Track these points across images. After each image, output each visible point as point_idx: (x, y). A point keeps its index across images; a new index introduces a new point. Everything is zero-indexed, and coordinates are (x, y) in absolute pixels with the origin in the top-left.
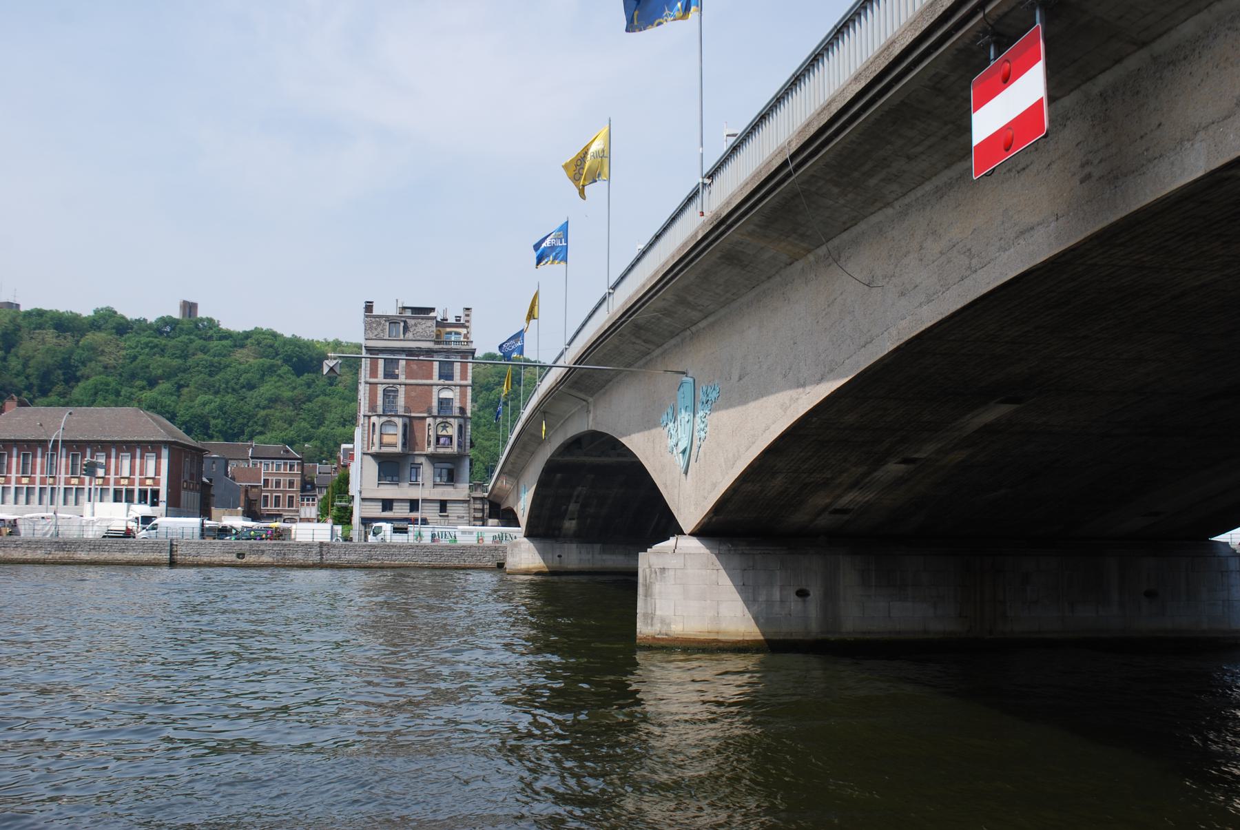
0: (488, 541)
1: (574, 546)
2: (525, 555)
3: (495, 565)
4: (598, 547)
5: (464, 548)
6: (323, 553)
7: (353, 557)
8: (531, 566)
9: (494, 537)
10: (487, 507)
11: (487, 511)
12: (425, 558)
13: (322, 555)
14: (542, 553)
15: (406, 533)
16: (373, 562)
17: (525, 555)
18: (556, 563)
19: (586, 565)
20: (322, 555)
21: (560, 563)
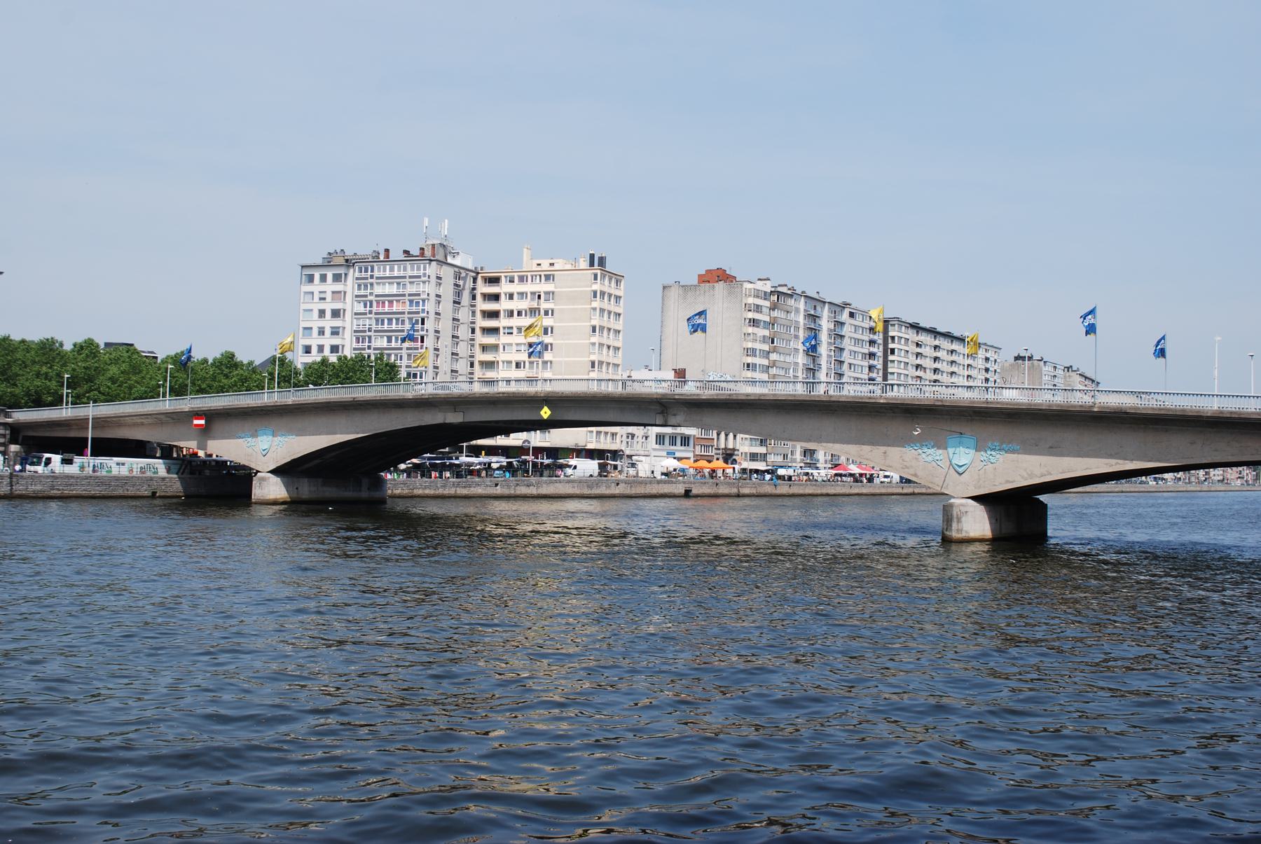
0: (89, 471)
1: (306, 480)
2: (272, 488)
3: (150, 494)
4: (320, 480)
5: (117, 478)
6: (14, 484)
7: (39, 488)
8: (278, 497)
9: (141, 468)
10: (8, 432)
11: (8, 437)
12: (97, 488)
13: (12, 486)
14: (287, 486)
15: (72, 464)
16: (55, 492)
17: (272, 488)
18: (295, 495)
19: (314, 496)
20: (12, 486)
21: (298, 494)
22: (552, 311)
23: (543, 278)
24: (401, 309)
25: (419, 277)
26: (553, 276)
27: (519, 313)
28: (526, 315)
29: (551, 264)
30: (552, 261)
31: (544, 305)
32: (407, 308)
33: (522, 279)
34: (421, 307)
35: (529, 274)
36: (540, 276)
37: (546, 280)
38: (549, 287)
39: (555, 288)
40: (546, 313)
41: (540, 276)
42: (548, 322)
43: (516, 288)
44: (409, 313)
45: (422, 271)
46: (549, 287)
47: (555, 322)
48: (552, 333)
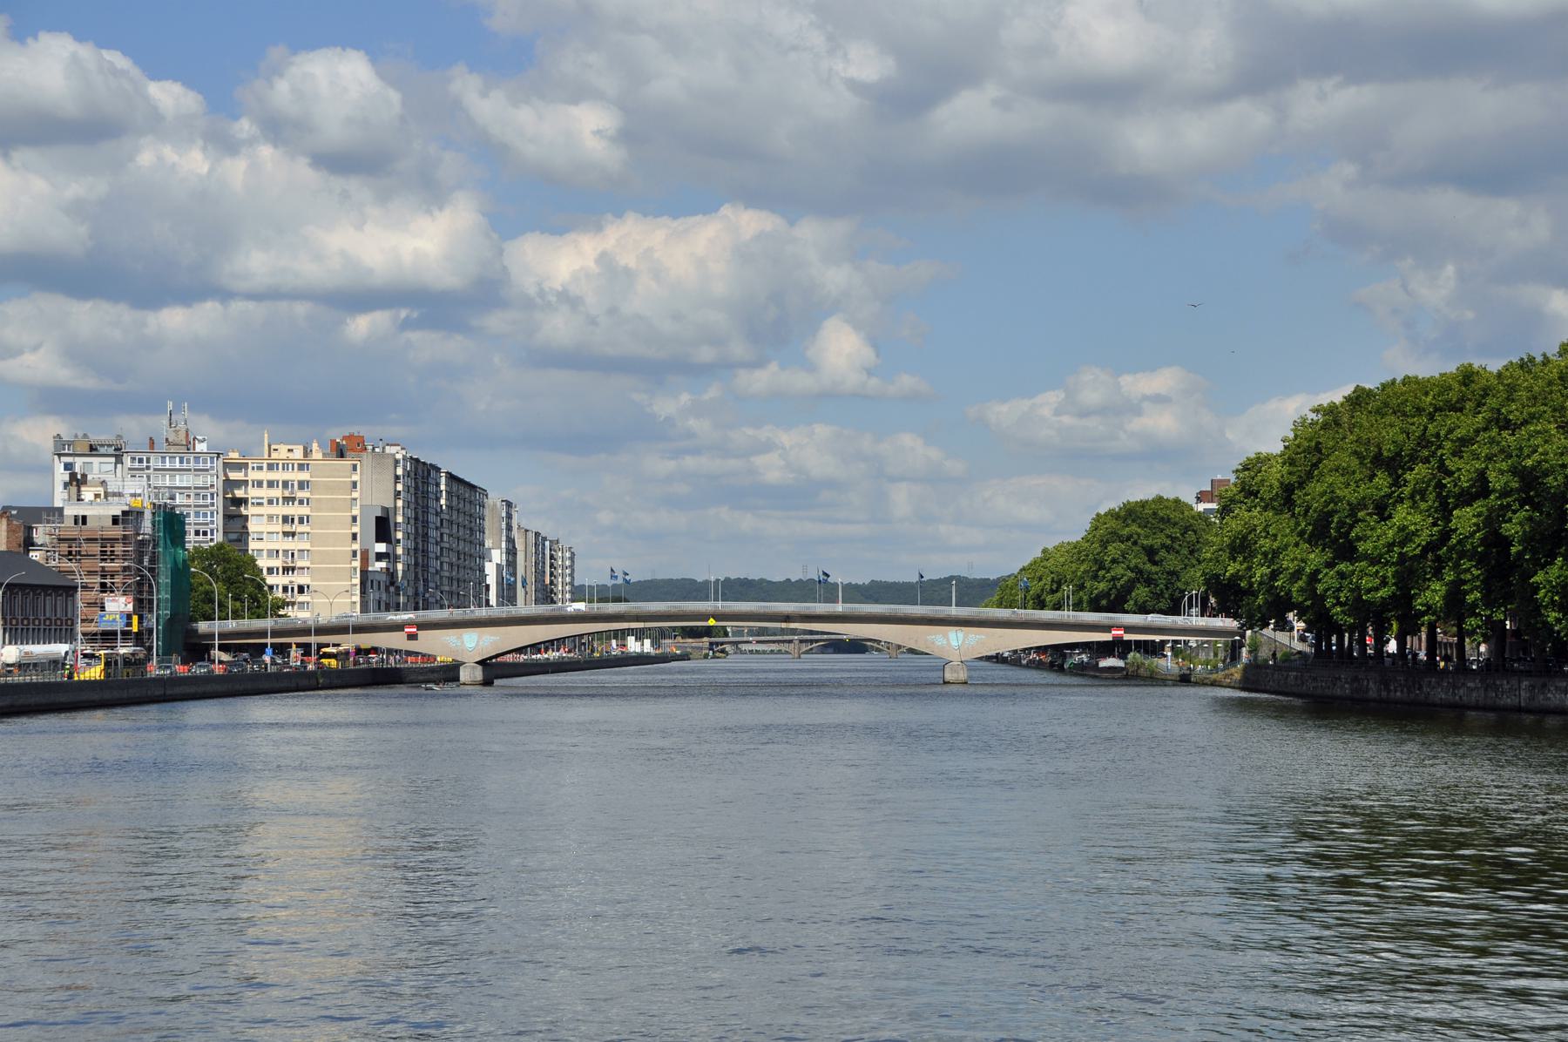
22: (308, 500)
23: (296, 466)
24: (185, 502)
25: (207, 470)
26: (308, 465)
27: (270, 502)
28: (277, 504)
29: (289, 450)
30: (290, 447)
31: (300, 494)
32: (191, 501)
33: (271, 467)
34: (209, 501)
35: (281, 462)
36: (293, 465)
37: (299, 469)
38: (304, 476)
39: (311, 477)
40: (301, 502)
41: (293, 465)
42: (304, 510)
43: (265, 476)
44: (195, 506)
45: (209, 465)
46: (304, 476)
47: (311, 511)
48: (308, 522)
